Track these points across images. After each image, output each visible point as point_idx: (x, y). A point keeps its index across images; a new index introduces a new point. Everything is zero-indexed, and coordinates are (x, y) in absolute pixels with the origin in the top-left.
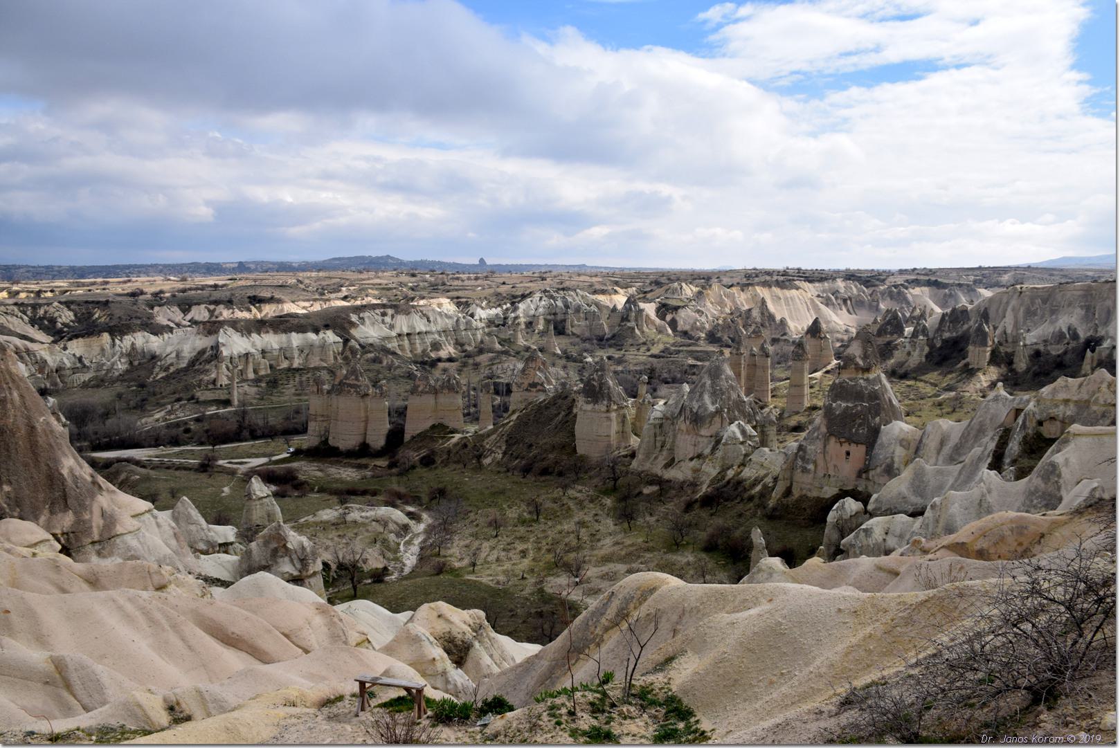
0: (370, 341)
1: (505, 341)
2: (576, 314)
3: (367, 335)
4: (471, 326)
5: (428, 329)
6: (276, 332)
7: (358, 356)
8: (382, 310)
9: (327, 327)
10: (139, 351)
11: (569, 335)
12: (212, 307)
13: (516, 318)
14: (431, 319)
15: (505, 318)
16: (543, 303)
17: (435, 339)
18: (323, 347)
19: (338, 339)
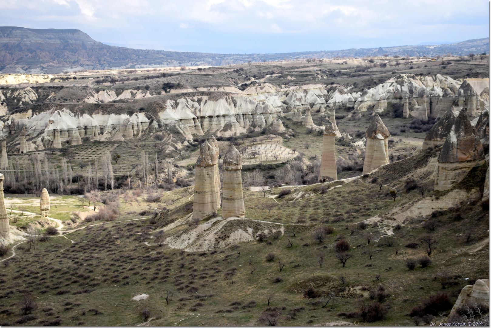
0: (168, 122)
1: (295, 124)
2: (419, 99)
3: (168, 117)
4: (267, 111)
5: (227, 113)
6: (103, 114)
7: (152, 134)
8: (200, 97)
9: (141, 110)
10: (16, 124)
11: (405, 118)
12: (135, 91)
13: (362, 102)
14: (237, 105)
15: (355, 102)
16: (391, 88)
17: (230, 121)
18: (126, 126)
19: (147, 120)
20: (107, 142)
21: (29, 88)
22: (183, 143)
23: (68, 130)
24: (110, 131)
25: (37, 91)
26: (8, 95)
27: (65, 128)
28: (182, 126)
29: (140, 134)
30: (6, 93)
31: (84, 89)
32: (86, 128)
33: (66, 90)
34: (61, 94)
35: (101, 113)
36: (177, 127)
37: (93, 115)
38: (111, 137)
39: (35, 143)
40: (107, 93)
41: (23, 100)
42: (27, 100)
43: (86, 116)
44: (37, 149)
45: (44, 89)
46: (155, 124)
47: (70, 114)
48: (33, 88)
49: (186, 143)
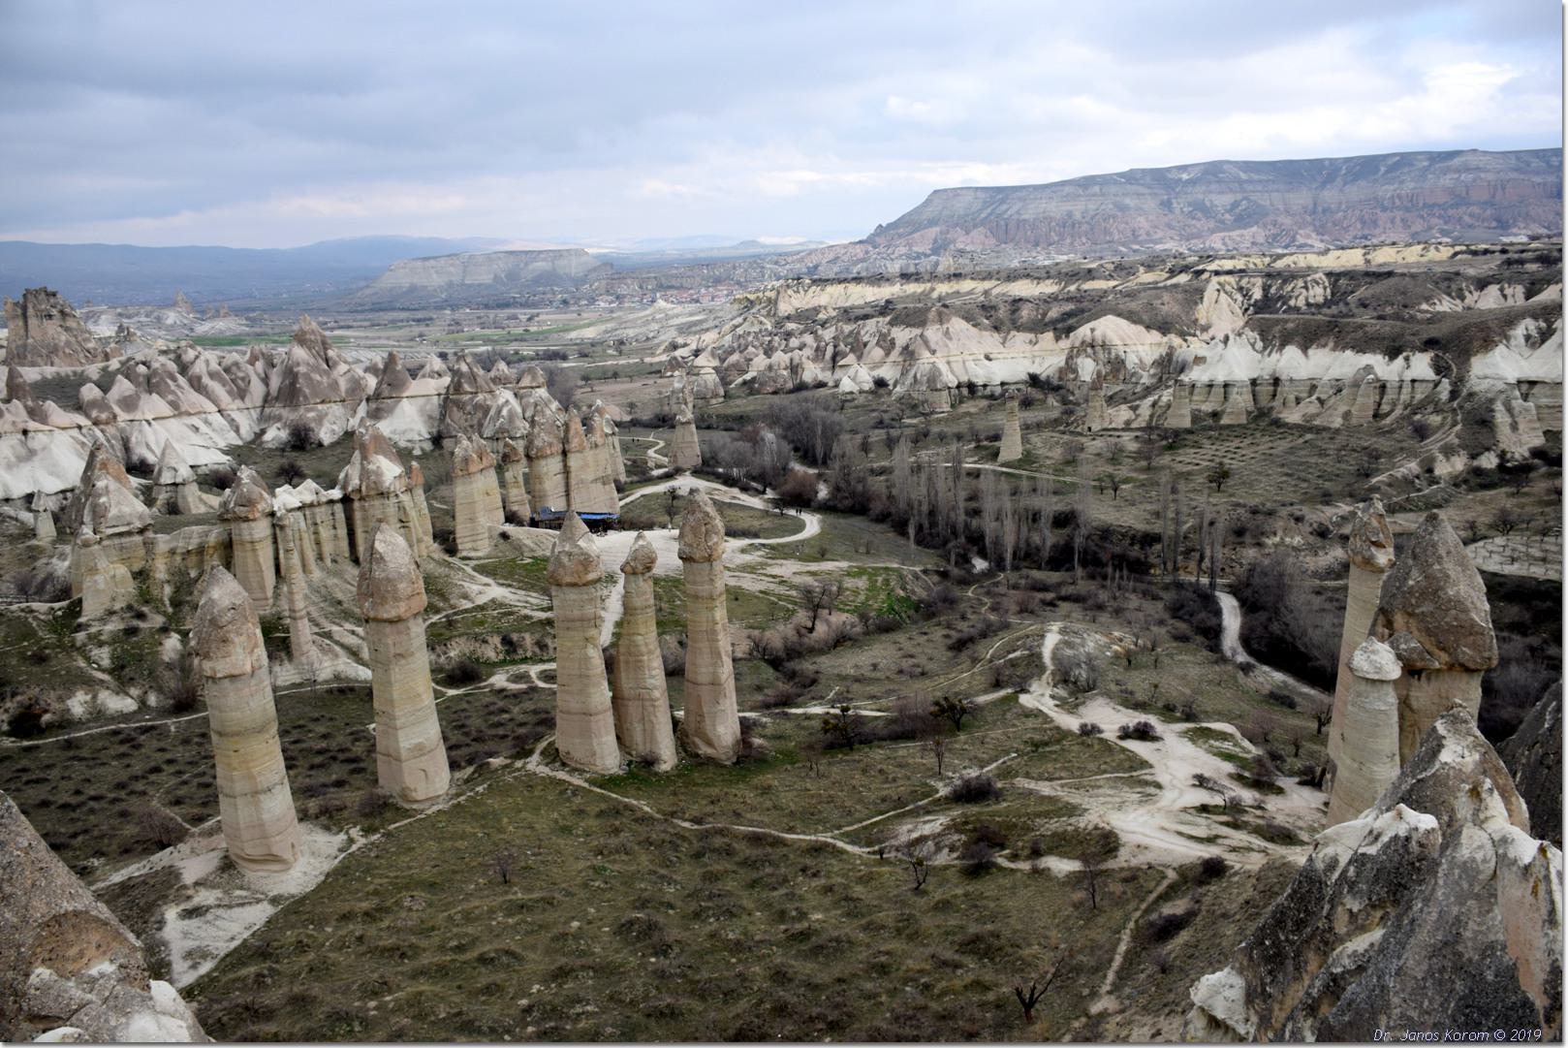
6: (1334, 349)
9: (1430, 344)
20: (1297, 426)
21: (1320, 276)
22: (1473, 457)
23: (1226, 385)
24: (1323, 397)
25: (1334, 285)
26: (1273, 290)
27: (1221, 378)
28: (1518, 403)
29: (1398, 411)
30: (1270, 286)
31: (1449, 279)
32: (1276, 381)
33: (1392, 281)
34: (1379, 287)
35: (1331, 344)
36: (1499, 406)
37: (1311, 352)
38: (1318, 415)
39: (1134, 409)
40: (1502, 290)
41: (1292, 303)
42: (1301, 302)
43: (1292, 352)
44: (1127, 427)
45: (1352, 278)
46: (1446, 386)
47: (1253, 345)
48: (1329, 275)
49: (1489, 461)
